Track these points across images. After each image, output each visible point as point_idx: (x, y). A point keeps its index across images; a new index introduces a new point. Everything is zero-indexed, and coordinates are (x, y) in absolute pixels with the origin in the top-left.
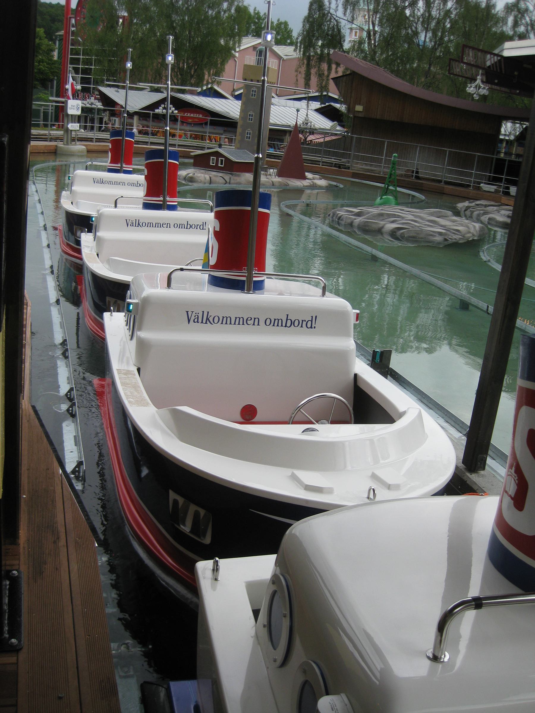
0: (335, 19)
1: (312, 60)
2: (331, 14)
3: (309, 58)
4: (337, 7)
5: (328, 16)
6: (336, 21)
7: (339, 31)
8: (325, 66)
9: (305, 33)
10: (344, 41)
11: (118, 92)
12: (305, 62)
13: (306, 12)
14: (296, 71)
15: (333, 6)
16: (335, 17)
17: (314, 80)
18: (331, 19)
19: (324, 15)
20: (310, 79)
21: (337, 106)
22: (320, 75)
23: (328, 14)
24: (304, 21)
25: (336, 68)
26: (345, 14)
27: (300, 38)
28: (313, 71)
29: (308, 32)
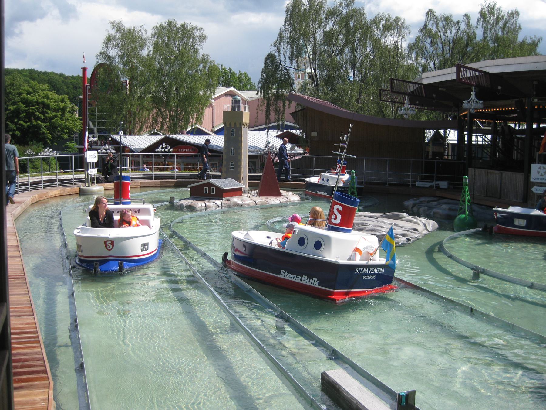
0: (285, 68)
1: (271, 100)
2: (282, 65)
3: (268, 99)
4: (285, 59)
5: (279, 67)
6: (286, 69)
7: (289, 76)
8: (280, 103)
9: (264, 81)
10: (294, 84)
11: (126, 138)
12: (266, 102)
13: (262, 66)
14: (257, 109)
15: (282, 58)
16: (285, 67)
17: (273, 115)
18: (282, 69)
19: (276, 66)
20: (270, 114)
21: (294, 131)
22: (277, 111)
23: (279, 65)
24: (262, 72)
25: (289, 104)
26: (291, 64)
27: (260, 85)
28: (272, 108)
29: (265, 80)
